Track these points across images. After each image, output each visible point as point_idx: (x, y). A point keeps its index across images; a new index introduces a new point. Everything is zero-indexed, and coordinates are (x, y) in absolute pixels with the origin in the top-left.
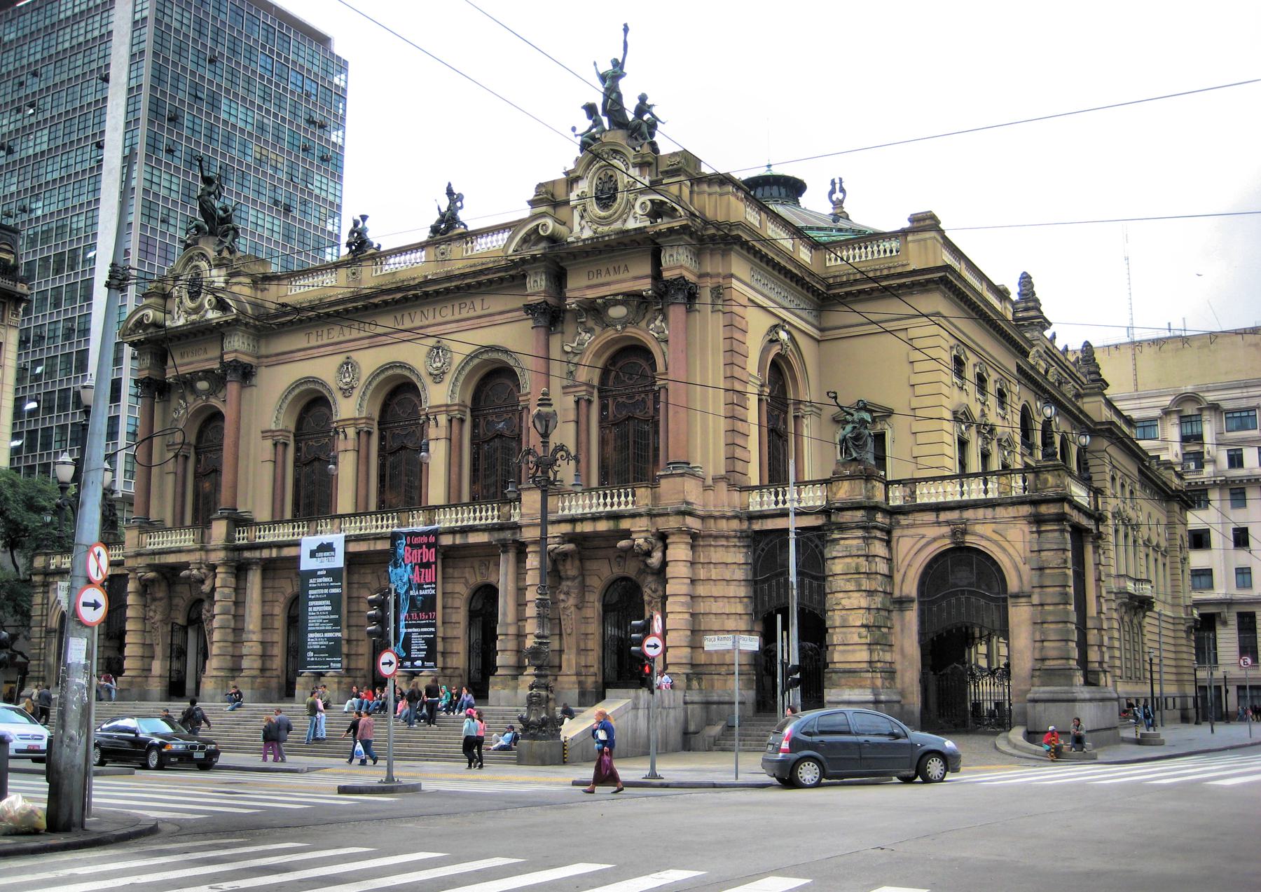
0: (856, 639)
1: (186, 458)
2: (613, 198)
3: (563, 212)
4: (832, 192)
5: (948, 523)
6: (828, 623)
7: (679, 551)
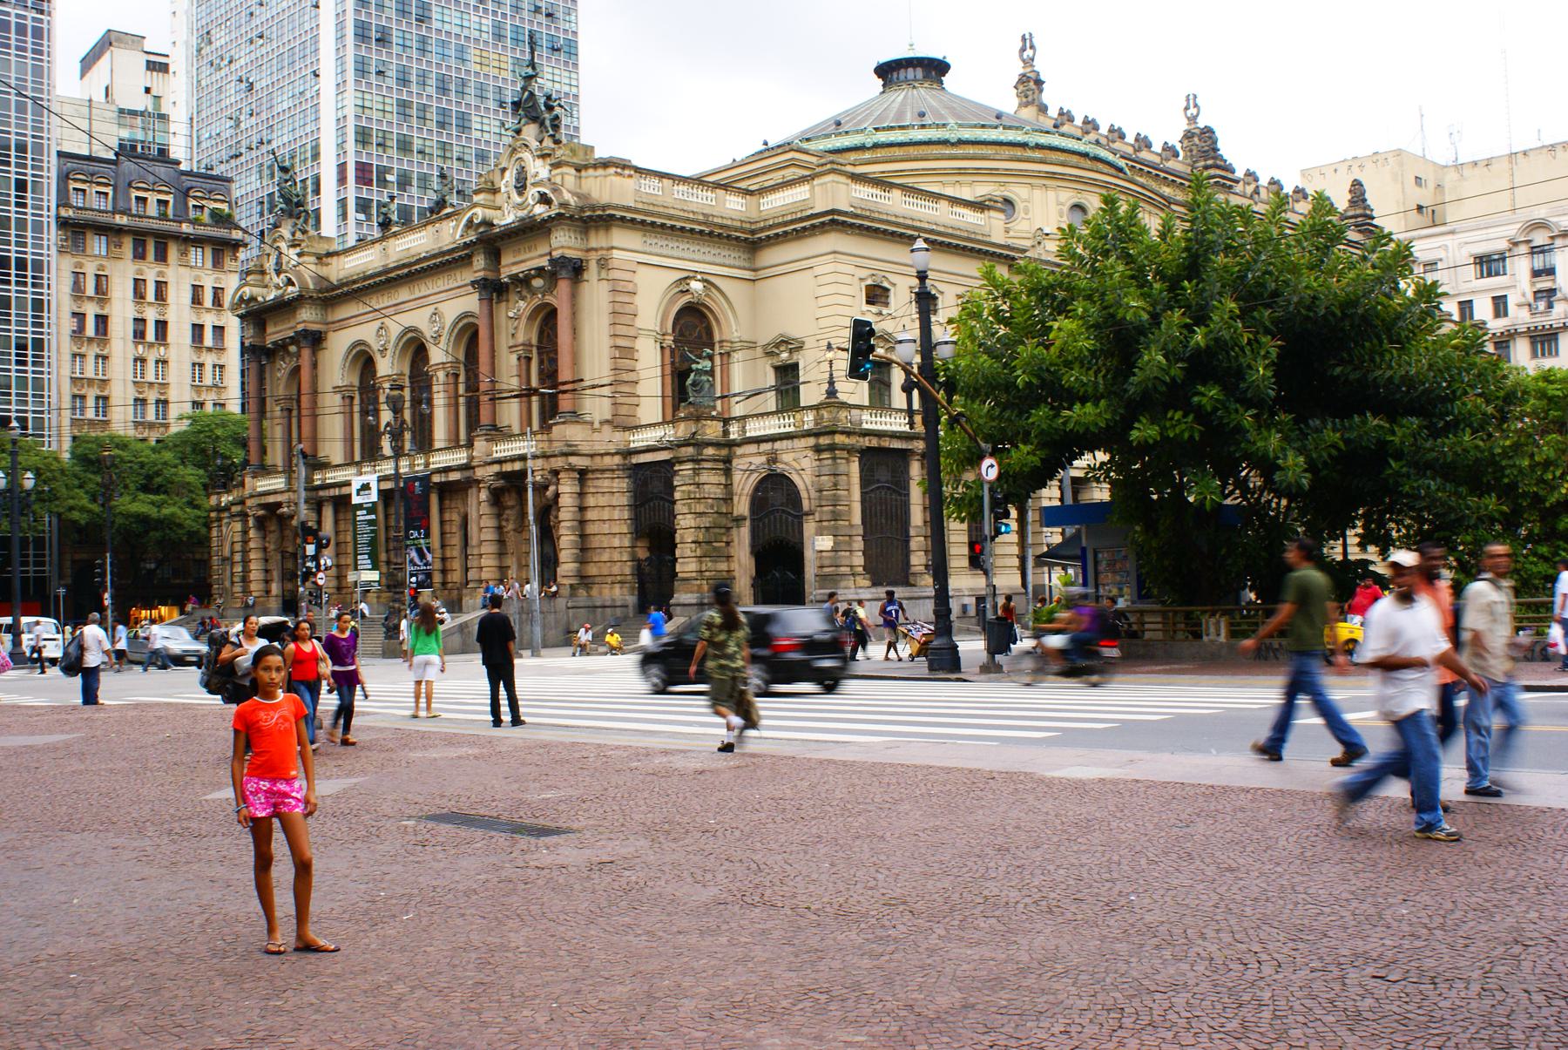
0: (689, 553)
4: (1023, 50)
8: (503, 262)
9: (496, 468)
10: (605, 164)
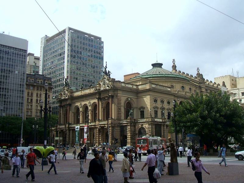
0: (129, 139)
2: (105, 84)
4: (173, 61)
8: (101, 95)
9: (100, 126)
10: (117, 81)
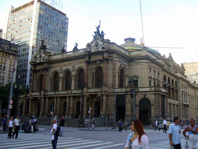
0: (129, 111)
1: (39, 81)
3: (91, 48)
4: (141, 40)
5: (143, 94)
6: (126, 108)
7: (105, 98)
9: (89, 94)
